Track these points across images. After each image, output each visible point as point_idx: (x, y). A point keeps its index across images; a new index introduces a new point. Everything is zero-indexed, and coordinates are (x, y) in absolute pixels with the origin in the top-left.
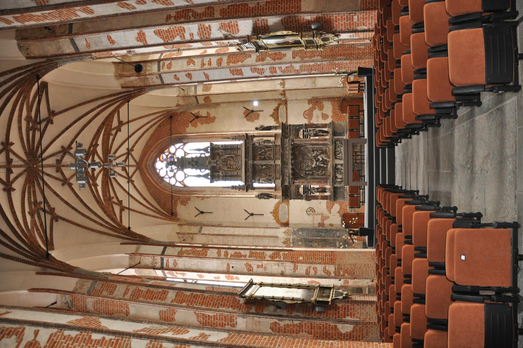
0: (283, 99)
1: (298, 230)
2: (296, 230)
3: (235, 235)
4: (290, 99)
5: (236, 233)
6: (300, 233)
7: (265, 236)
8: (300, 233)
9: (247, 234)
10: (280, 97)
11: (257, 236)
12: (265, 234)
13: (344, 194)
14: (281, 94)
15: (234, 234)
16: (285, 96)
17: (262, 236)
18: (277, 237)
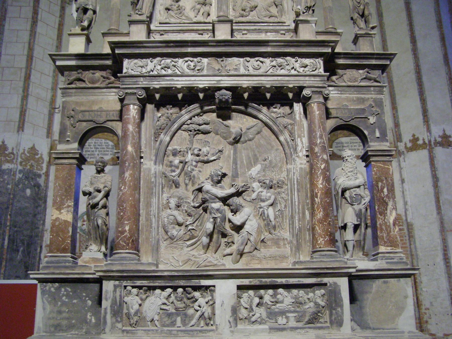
0: (401, 146)
1: (38, 186)
2: (41, 181)
3: (34, 22)
4: (403, 164)
5: (40, 28)
6: (28, 192)
7: (25, 97)
8: (28, 192)
9: (35, 54)
10: (407, 138)
11: (28, 77)
12: (31, 100)
13: (71, 327)
14: (415, 140)
15: (39, 24)
16: (410, 150)
17: (26, 89)
18: (21, 128)
